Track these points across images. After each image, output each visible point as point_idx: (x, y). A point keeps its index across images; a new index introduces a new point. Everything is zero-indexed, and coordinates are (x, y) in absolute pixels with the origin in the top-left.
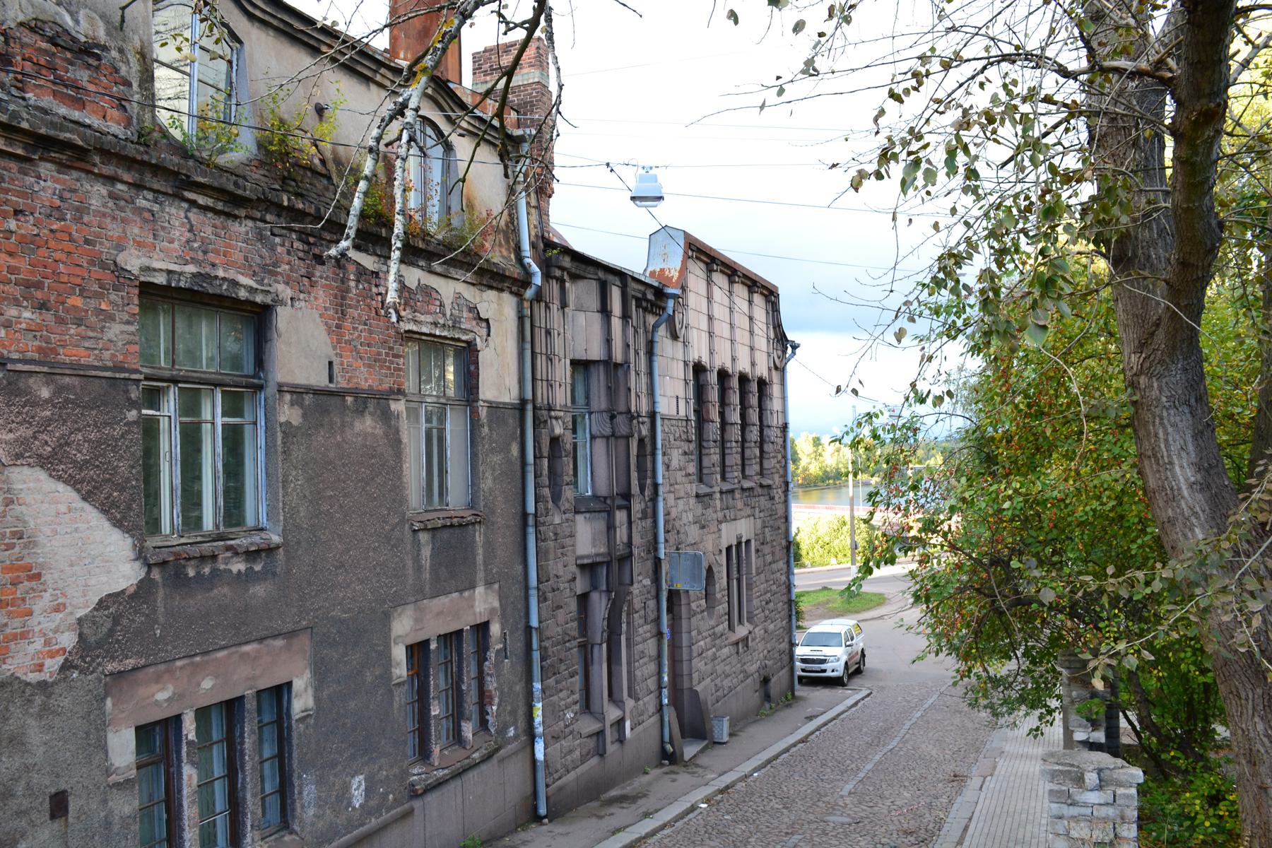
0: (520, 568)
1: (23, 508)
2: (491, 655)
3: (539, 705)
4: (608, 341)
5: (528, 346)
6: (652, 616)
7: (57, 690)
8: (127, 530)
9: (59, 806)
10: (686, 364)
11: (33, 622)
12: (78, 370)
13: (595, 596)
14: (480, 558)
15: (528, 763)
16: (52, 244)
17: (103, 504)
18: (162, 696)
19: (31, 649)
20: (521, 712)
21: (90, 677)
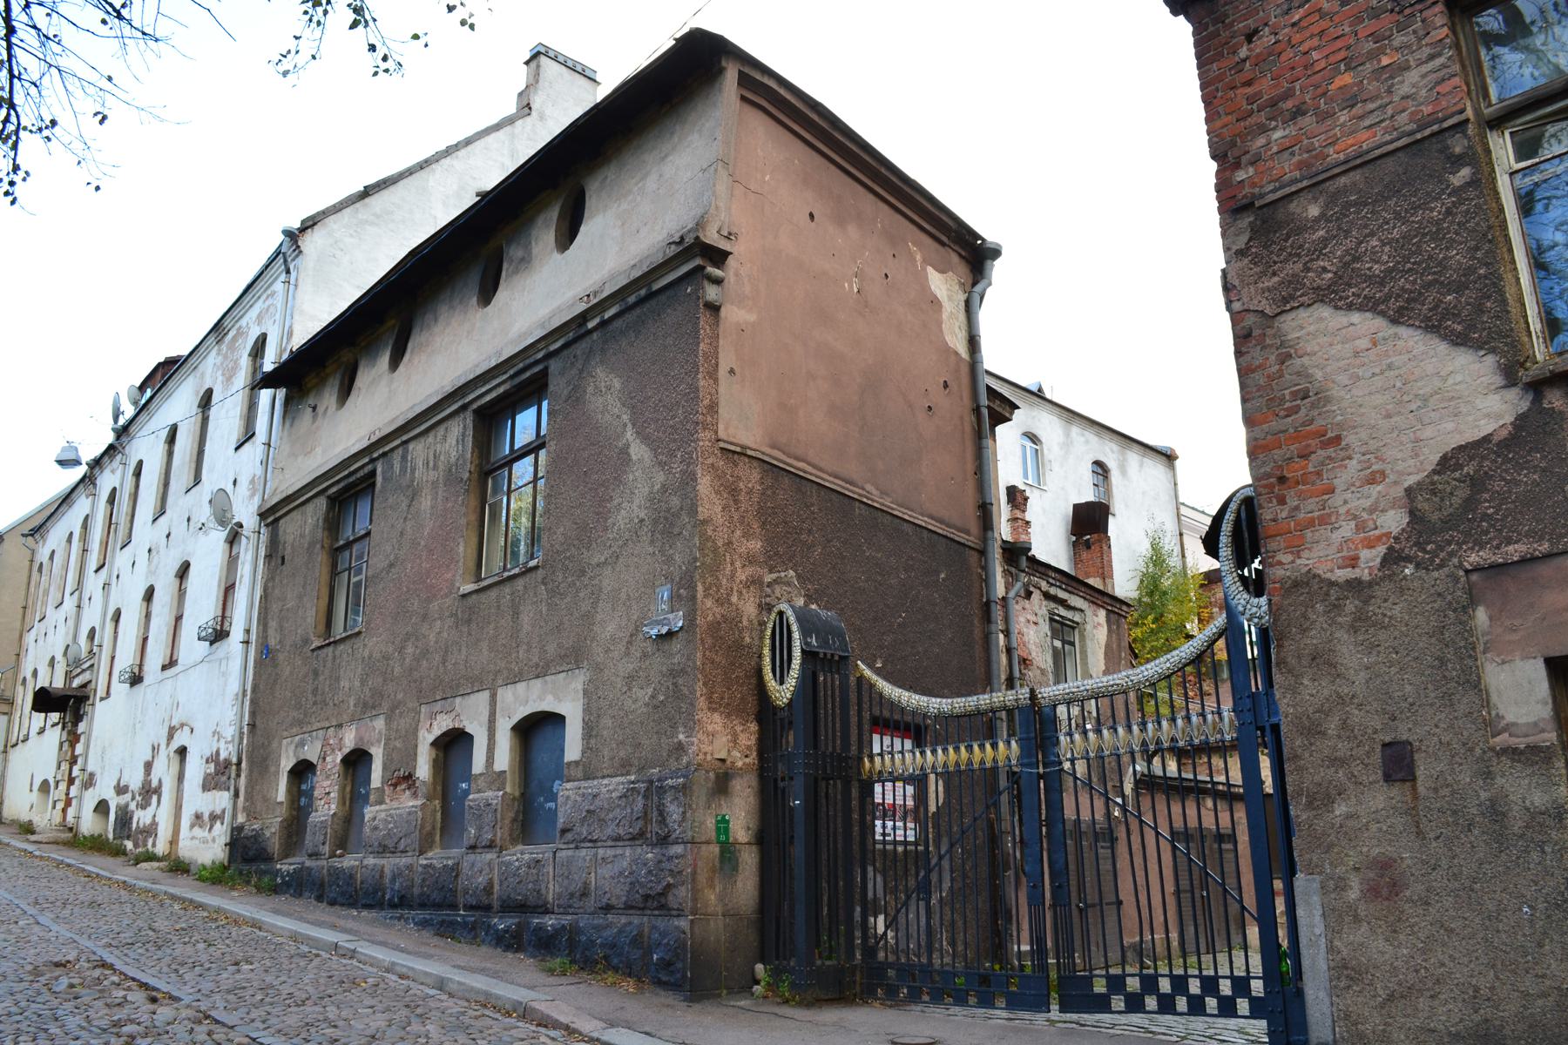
1: (1305, 360)
7: (1379, 592)
8: (1478, 346)
9: (1398, 763)
11: (1336, 500)
12: (1363, 162)
16: (1297, 38)
17: (1429, 319)
19: (1337, 537)
21: (1436, 574)
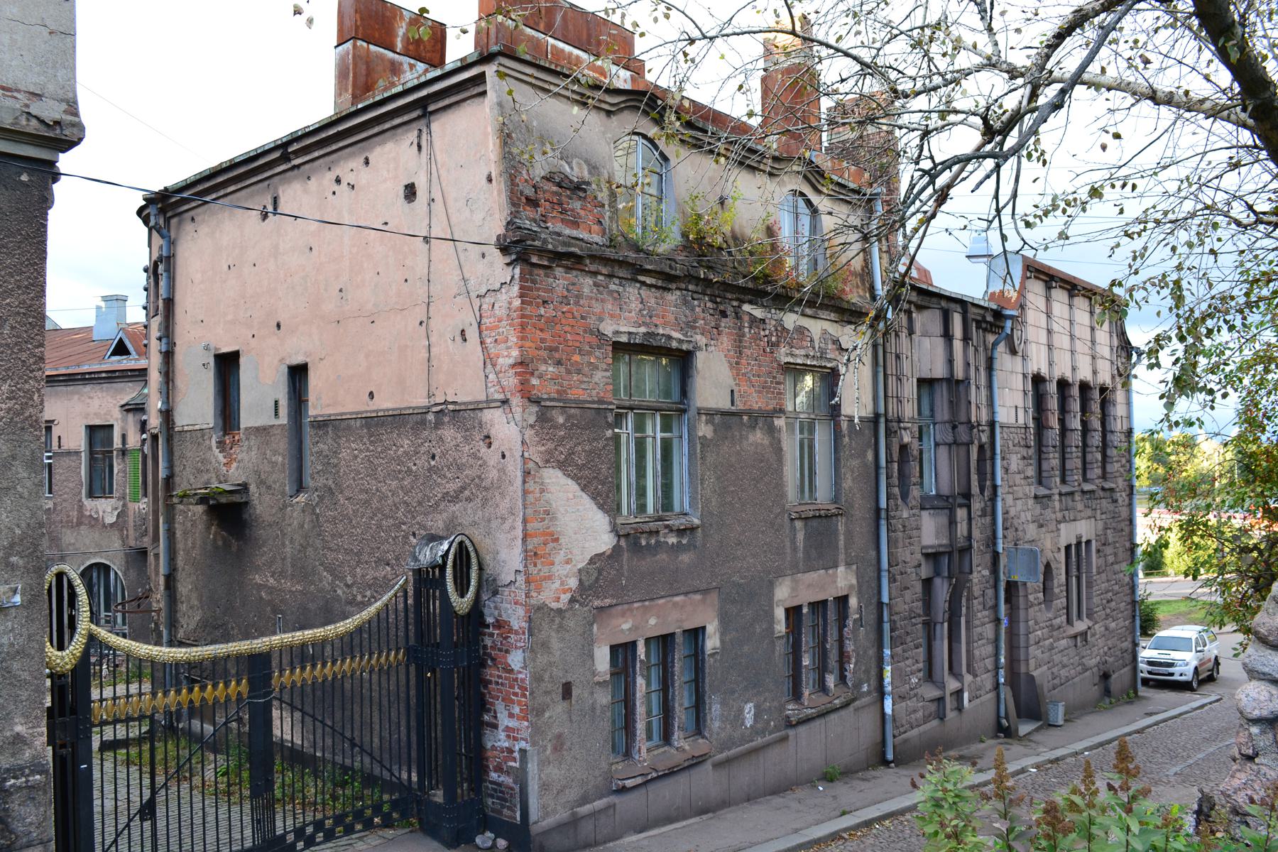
0: (874, 553)
2: (850, 622)
3: (889, 668)
4: (950, 361)
5: (881, 369)
6: (990, 603)
8: (606, 512)
9: (567, 691)
10: (1025, 376)
11: (554, 569)
12: (580, 405)
13: (938, 581)
14: (841, 543)
15: (878, 716)
16: (563, 321)
18: (625, 626)
20: (873, 672)
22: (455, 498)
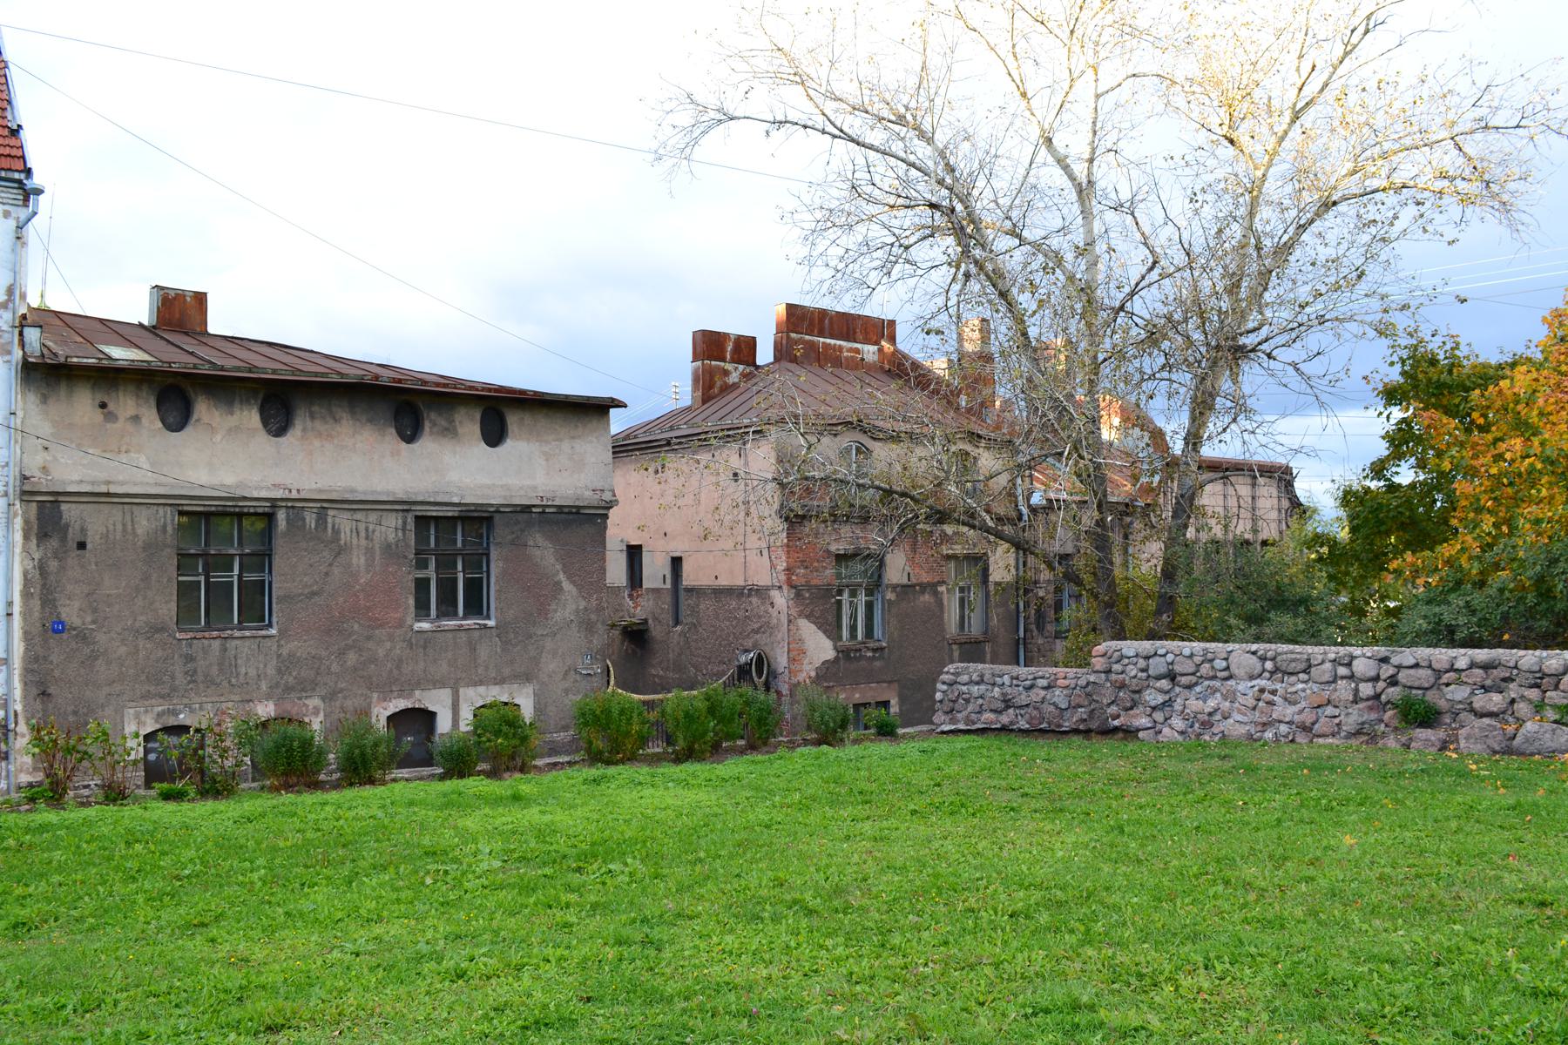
22: (757, 632)
